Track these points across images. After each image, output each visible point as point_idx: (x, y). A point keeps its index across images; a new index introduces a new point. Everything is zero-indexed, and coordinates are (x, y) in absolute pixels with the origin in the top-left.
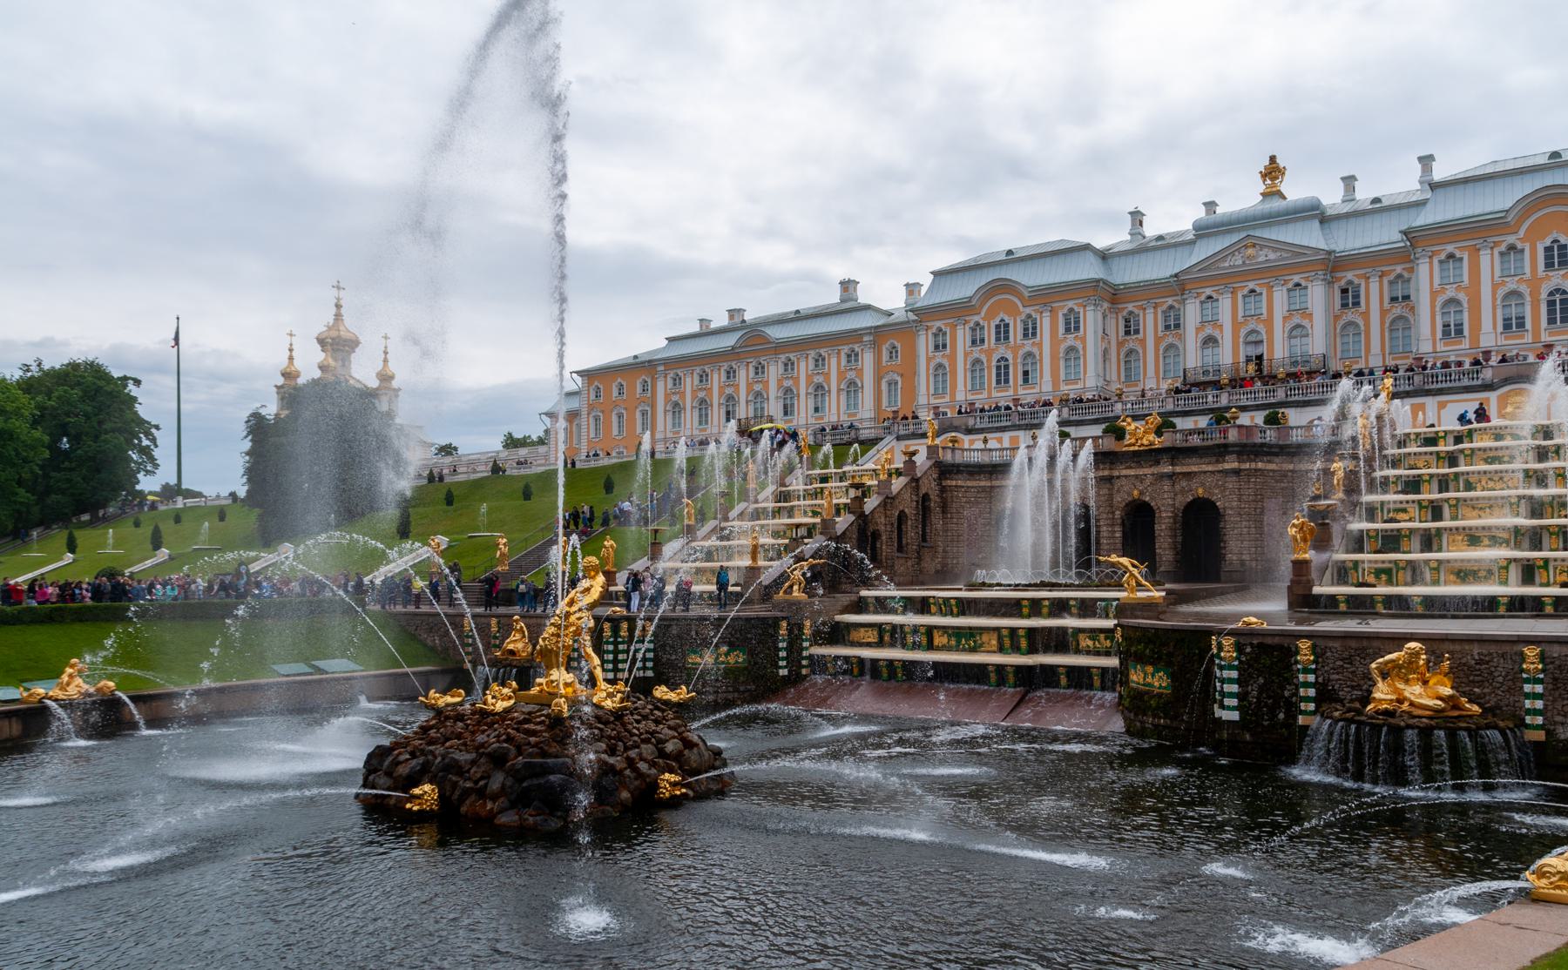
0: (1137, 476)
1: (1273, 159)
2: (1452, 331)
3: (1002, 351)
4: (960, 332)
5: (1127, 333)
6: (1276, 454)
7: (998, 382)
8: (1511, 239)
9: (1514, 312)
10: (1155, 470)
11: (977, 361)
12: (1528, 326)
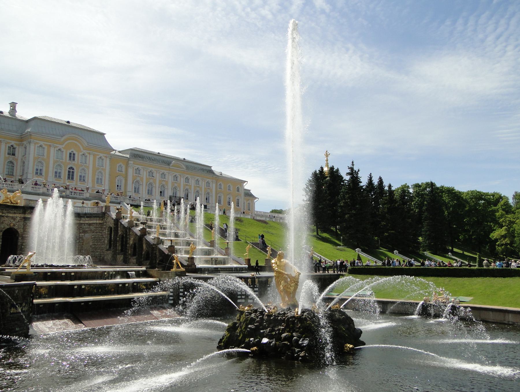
0: (12, 218)
9: (59, 171)
10: (22, 216)
12: (62, 177)
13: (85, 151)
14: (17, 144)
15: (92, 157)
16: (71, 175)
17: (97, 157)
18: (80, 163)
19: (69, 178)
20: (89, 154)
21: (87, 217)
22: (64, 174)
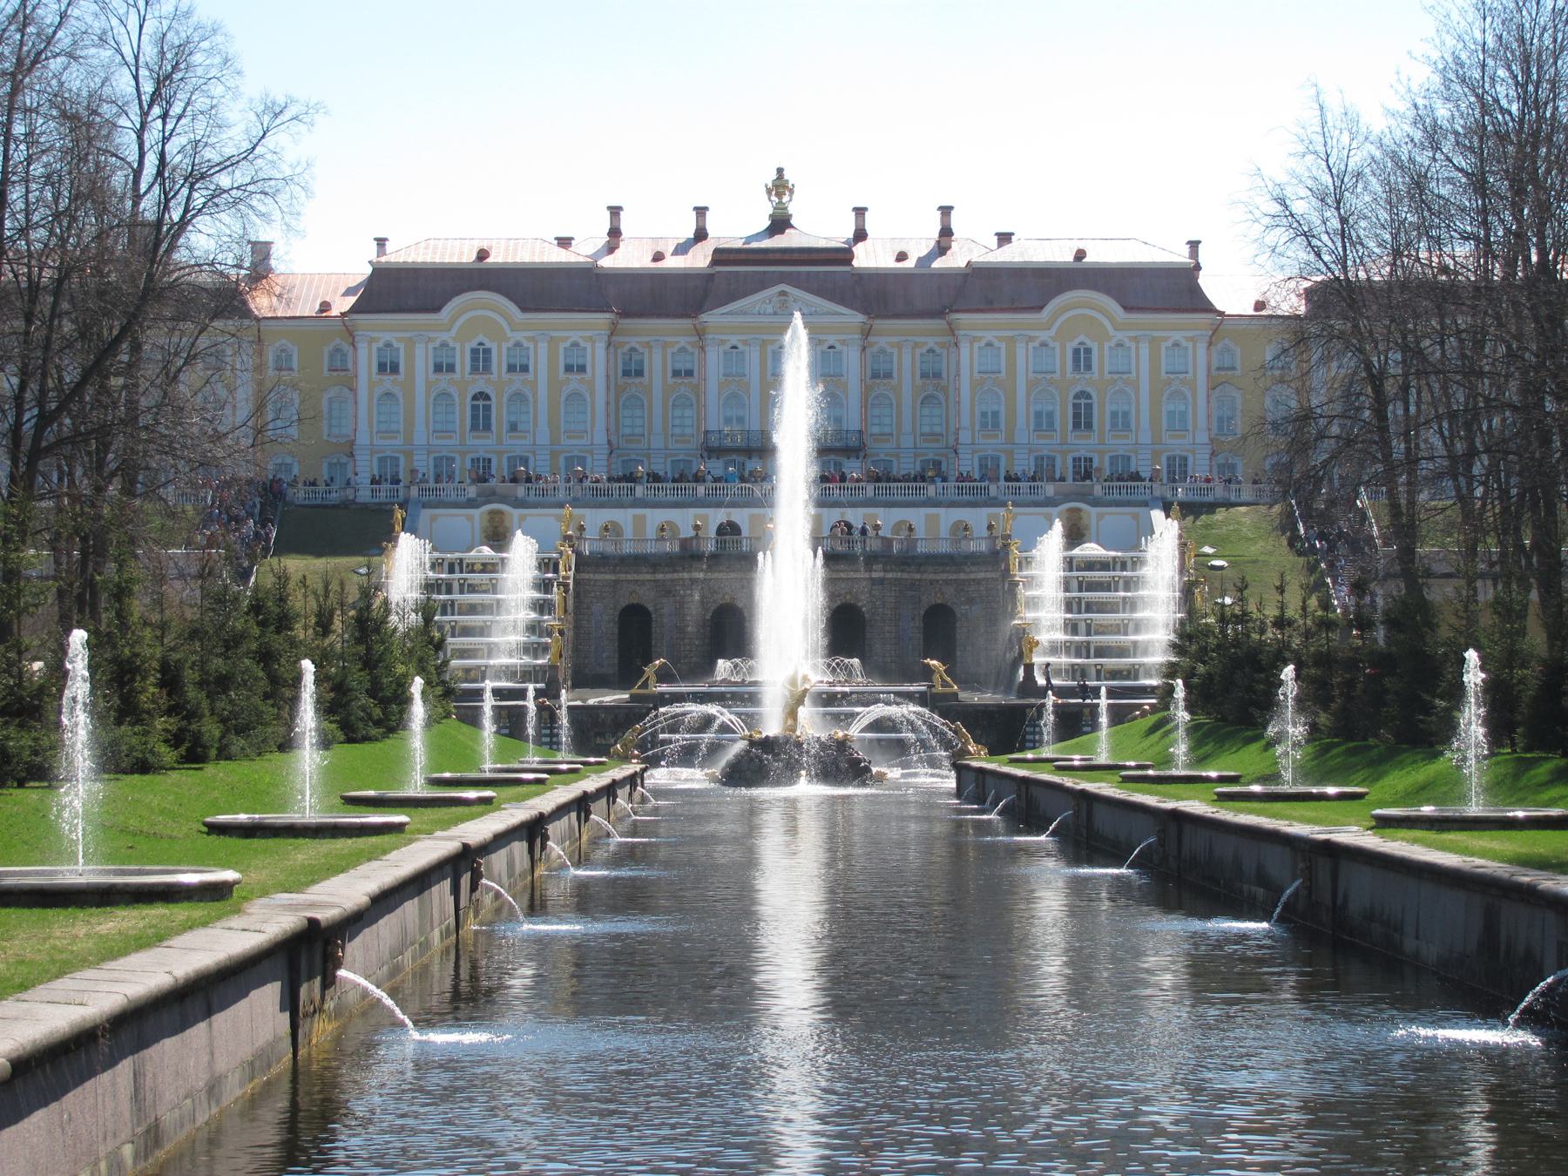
1: (780, 171)
2: (990, 422)
3: (480, 384)
4: (420, 351)
5: (626, 373)
6: (909, 565)
7: (474, 427)
8: (1044, 336)
11: (445, 395)
12: (1057, 426)
13: (1120, 336)
14: (942, 345)
15: (1145, 350)
16: (1082, 419)
17: (1164, 345)
18: (1108, 377)
19: (1076, 425)
20: (1136, 339)
21: (973, 564)
22: (1063, 415)
